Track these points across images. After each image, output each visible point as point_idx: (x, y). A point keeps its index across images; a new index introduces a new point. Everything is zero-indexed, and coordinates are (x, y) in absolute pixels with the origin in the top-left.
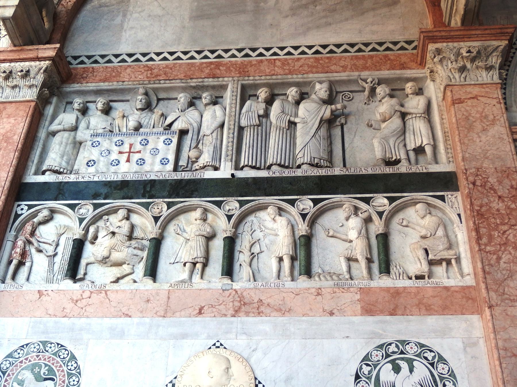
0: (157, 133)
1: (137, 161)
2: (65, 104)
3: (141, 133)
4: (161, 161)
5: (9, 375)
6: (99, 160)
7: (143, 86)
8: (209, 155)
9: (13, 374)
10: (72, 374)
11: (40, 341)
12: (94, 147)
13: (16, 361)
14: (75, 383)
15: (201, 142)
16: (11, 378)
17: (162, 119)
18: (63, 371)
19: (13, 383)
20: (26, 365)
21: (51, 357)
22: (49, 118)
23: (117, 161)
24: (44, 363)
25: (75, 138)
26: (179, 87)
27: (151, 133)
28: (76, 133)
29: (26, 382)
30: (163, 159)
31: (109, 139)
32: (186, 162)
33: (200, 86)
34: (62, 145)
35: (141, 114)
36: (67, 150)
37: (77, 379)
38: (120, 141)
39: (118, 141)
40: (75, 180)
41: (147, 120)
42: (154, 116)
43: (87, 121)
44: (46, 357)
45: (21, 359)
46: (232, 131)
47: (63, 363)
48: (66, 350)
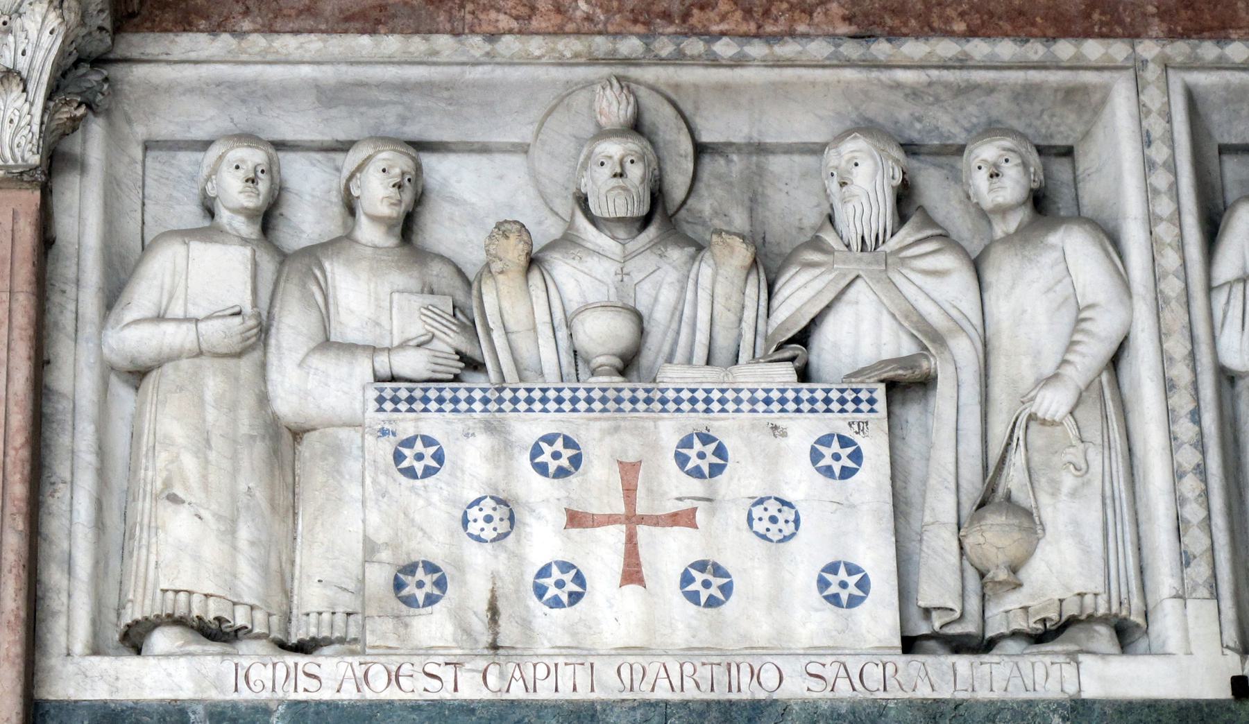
0: (761, 395)
1: (686, 579)
2: (138, 152)
3: (671, 395)
4: (823, 584)
6: (460, 566)
7: (620, 70)
8: (1086, 551)
12: (410, 473)
15: (1017, 459)
17: (751, 290)
22: (92, 274)
23: (568, 577)
25: (264, 399)
26: (827, 84)
27: (730, 395)
28: (263, 366)
30: (833, 568)
31: (489, 428)
32: (953, 581)
33: (947, 85)
34: (212, 456)
35: (626, 258)
36: (243, 487)
38: (559, 445)
39: (550, 439)
40: (349, 694)
41: (668, 296)
42: (705, 271)
43: (315, 289)
46: (1183, 402)
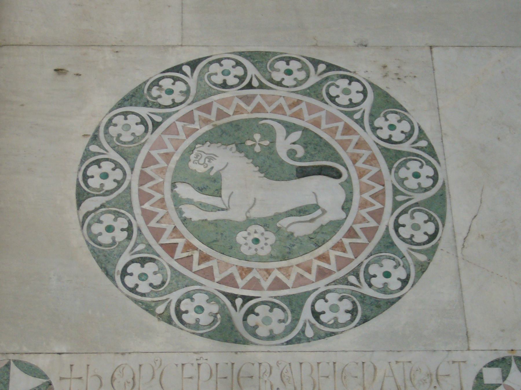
5: (150, 160)
9: (167, 157)
10: (399, 154)
11: (240, 54)
13: (166, 116)
14: (427, 183)
16: (162, 171)
18: (361, 144)
19: (173, 185)
20: (207, 128)
21: (299, 102)
24: (279, 122)
29: (225, 183)
37: (428, 171)
44: (282, 101)
45: (183, 110)
47: (356, 121)
48: (351, 79)
